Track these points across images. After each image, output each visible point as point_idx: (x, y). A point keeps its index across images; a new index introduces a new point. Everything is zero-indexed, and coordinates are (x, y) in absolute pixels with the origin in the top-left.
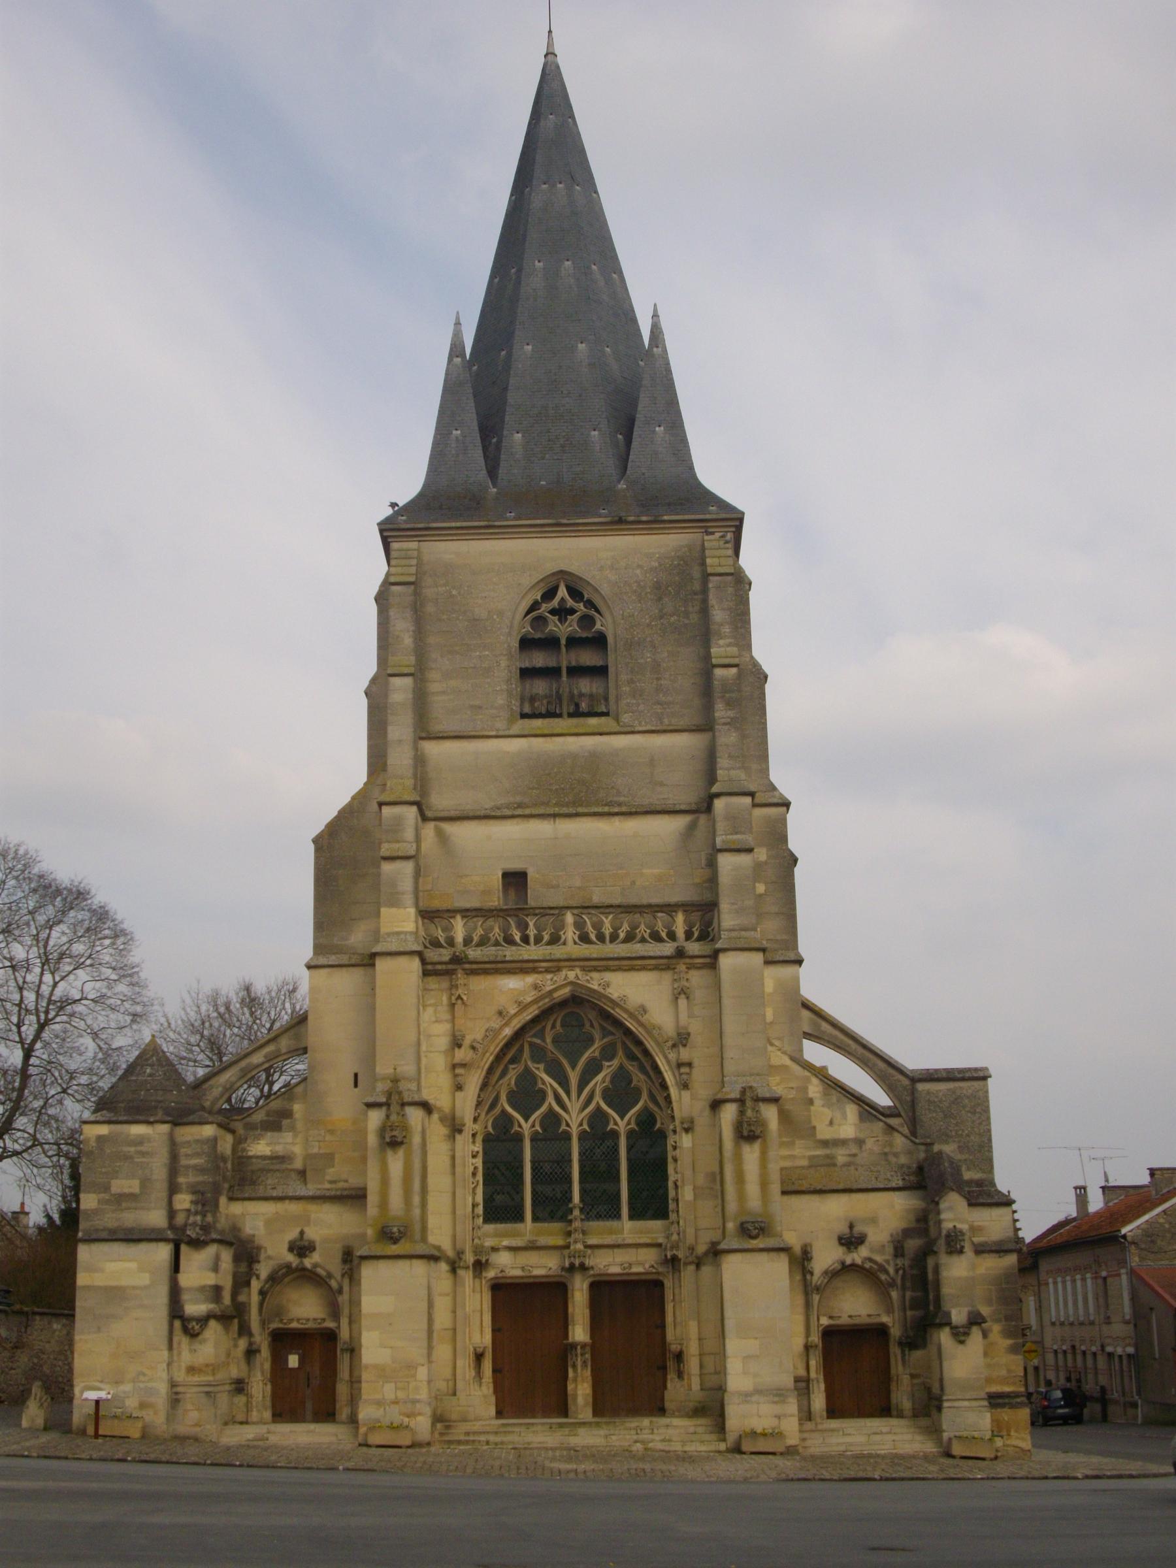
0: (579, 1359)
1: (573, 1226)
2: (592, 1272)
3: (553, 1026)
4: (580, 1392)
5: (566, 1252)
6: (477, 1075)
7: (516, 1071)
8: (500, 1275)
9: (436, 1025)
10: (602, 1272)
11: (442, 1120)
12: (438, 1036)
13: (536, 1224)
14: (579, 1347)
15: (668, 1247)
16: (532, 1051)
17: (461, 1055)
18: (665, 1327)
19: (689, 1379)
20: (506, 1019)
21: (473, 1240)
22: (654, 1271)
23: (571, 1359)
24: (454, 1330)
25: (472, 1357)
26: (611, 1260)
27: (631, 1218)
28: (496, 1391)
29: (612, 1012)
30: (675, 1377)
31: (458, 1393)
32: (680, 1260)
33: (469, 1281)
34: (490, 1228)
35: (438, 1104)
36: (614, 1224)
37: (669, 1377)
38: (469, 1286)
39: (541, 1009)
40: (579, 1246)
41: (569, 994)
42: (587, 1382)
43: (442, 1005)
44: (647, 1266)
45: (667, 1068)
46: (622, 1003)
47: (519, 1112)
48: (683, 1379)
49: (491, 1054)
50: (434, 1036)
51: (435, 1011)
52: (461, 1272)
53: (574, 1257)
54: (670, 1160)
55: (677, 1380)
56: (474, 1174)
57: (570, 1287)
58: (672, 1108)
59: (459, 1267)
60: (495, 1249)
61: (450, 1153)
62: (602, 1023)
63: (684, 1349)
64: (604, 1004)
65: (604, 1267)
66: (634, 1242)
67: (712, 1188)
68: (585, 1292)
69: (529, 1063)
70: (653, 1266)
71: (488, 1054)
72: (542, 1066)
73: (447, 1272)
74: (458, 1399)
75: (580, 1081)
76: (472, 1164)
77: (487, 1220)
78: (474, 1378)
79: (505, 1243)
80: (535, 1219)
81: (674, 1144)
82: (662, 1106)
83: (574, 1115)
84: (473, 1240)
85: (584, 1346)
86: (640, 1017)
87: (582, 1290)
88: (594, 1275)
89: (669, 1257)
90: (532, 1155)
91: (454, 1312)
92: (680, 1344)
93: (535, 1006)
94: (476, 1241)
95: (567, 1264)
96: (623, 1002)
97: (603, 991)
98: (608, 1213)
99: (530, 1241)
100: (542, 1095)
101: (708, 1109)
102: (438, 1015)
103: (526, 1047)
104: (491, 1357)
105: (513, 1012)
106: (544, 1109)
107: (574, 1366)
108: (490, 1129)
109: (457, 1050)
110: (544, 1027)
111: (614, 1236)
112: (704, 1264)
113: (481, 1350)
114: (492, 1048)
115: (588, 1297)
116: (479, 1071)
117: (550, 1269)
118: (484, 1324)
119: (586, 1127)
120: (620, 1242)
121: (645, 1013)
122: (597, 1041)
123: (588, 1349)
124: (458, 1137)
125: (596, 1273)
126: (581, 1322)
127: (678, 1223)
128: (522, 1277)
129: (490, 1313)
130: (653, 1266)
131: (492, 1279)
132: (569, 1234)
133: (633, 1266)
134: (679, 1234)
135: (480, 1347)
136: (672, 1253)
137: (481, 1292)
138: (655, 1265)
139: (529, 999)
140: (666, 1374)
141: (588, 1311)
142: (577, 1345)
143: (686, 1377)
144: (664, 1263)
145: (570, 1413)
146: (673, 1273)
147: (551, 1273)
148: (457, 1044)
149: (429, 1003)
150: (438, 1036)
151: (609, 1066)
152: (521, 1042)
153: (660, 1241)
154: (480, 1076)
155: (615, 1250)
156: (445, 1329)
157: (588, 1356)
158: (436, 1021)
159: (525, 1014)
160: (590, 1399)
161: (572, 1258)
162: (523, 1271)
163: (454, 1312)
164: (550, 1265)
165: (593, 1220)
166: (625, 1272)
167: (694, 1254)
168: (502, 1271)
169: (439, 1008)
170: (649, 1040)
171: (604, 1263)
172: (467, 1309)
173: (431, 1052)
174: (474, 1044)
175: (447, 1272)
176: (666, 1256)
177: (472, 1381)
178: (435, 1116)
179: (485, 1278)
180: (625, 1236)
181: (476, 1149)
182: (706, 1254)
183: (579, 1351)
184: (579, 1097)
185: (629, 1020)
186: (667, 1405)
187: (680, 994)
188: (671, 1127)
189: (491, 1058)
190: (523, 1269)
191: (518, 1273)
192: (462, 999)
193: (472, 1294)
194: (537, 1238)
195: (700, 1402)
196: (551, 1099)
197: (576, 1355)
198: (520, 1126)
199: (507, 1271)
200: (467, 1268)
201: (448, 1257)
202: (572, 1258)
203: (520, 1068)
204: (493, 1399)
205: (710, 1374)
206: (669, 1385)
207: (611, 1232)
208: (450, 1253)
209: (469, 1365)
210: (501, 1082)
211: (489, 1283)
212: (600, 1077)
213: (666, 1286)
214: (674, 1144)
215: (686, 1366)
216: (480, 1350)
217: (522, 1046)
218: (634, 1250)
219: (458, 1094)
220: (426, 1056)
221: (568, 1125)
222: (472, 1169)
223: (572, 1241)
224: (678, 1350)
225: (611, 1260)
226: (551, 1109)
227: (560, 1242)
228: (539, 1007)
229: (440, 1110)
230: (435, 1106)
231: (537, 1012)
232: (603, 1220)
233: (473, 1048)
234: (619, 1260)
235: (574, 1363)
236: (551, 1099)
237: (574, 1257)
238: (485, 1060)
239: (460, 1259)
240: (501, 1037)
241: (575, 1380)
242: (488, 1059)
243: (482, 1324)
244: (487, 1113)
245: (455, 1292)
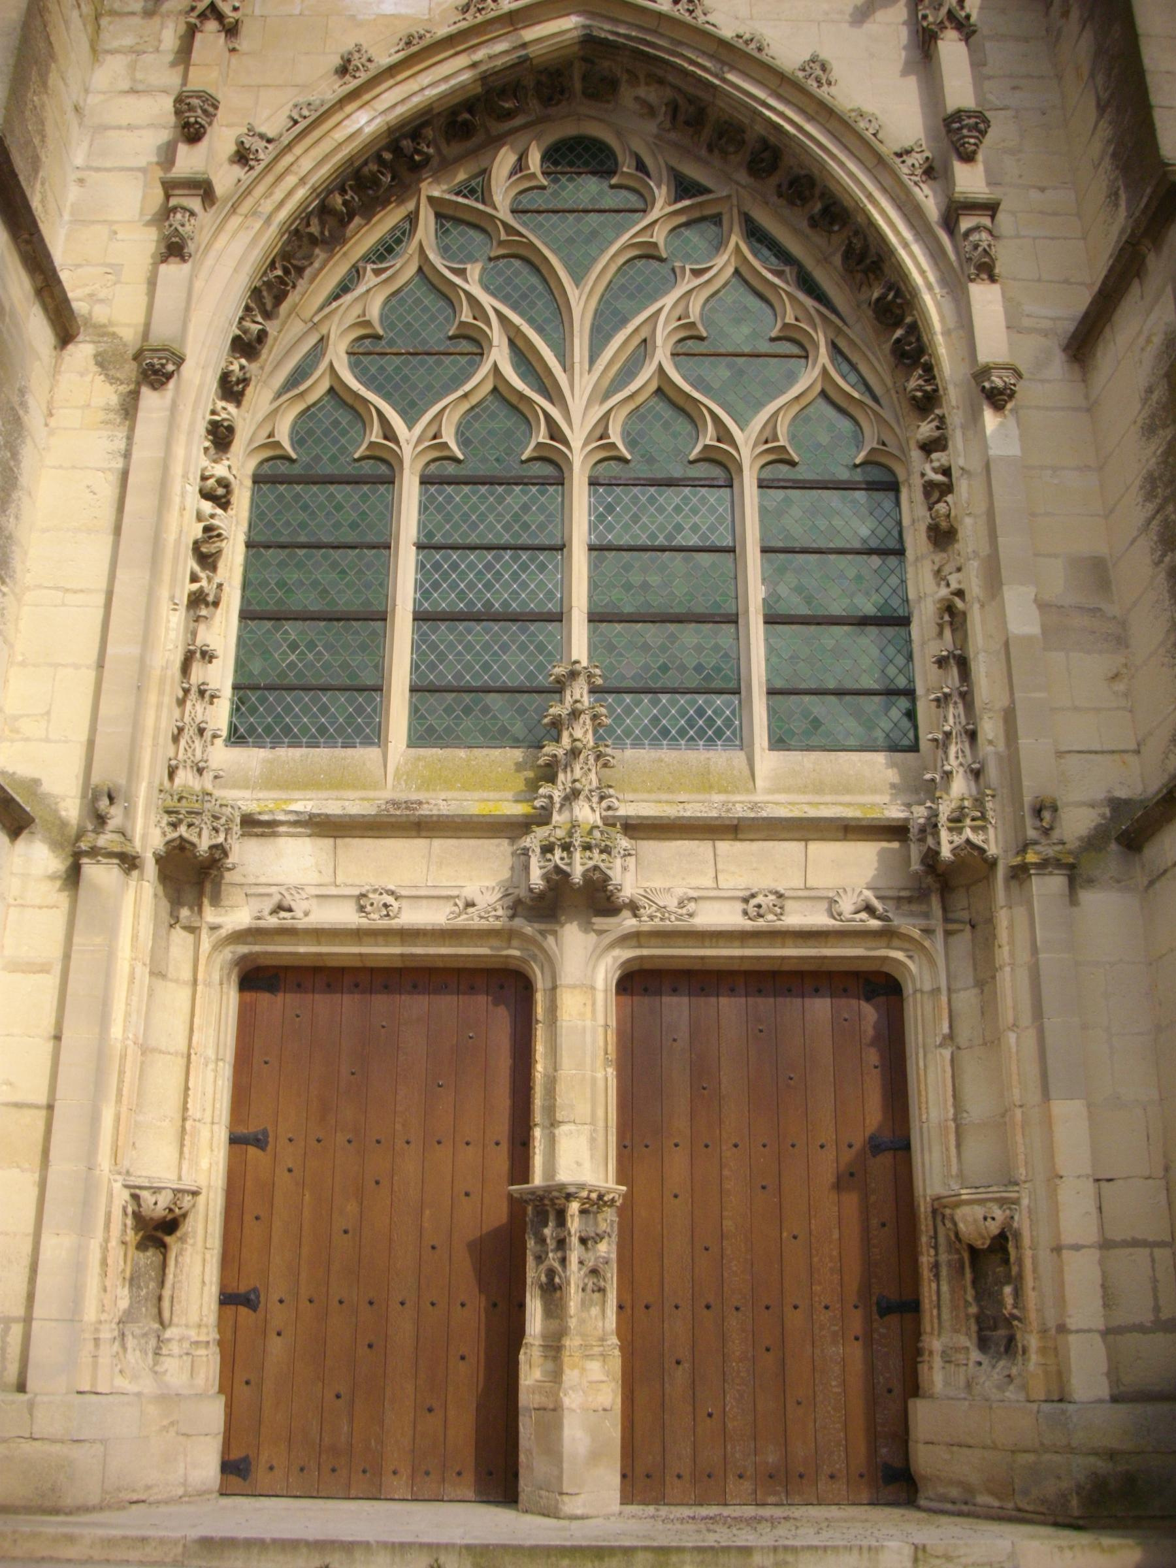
0: (574, 1257)
1: (566, 740)
2: (628, 922)
3: (520, 165)
4: (571, 1400)
5: (534, 840)
6: (245, 238)
7: (384, 276)
8: (272, 921)
9: (132, 100)
10: (671, 923)
11: (102, 362)
12: (130, 127)
13: (422, 752)
14: (574, 1207)
15: (943, 819)
16: (442, 232)
17: (189, 161)
18: (907, 1147)
19: (1054, 1351)
20: (363, 77)
21: (172, 774)
22: (874, 923)
23: (539, 1259)
24: (50, 1107)
25: (121, 1228)
26: (708, 882)
27: (779, 742)
28: (227, 1385)
29: (717, 82)
30: (966, 1341)
31: (30, 1385)
32: (992, 864)
33: (136, 916)
34: (253, 758)
35: (100, 314)
36: (720, 759)
37: (935, 1343)
38: (135, 937)
39: (483, 68)
40: (586, 813)
41: (575, 33)
42: (604, 1356)
43: (157, 50)
44: (847, 906)
45: (908, 235)
46: (751, 49)
47: (387, 397)
48: (1010, 1347)
49: (303, 181)
50: (120, 128)
51: (132, 67)
52: (101, 874)
53: (566, 847)
54: (916, 541)
55: (975, 1355)
56: (207, 559)
57: (541, 983)
58: (929, 369)
59: (94, 852)
60: (252, 825)
61: (119, 464)
62: (674, 163)
63: (1022, 1222)
64: (692, 62)
65: (681, 904)
66: (796, 813)
67: (1095, 611)
68: (600, 996)
69: (433, 256)
70: (869, 909)
71: (291, 180)
72: (474, 271)
73: (52, 878)
74: (31, 1406)
75: (598, 314)
76: (199, 518)
77: (236, 737)
78: (126, 1319)
79: (305, 804)
80: (421, 736)
81: (940, 478)
82: (878, 390)
83: (576, 405)
84: (172, 774)
85: (594, 1204)
86: (812, 85)
87: (593, 988)
88: (635, 938)
89: (946, 852)
90: (422, 525)
91: (58, 1038)
92: (1002, 1202)
93: (462, 61)
94: (184, 777)
95: (536, 877)
96: (753, 46)
97: (687, 18)
98: (691, 723)
99: (395, 804)
100: (475, 343)
101: (1059, 359)
102: (139, 76)
103: (427, 218)
104: (215, 1242)
105: (385, 60)
106: (479, 380)
107: (552, 1289)
108: (283, 435)
109: (182, 149)
110: (485, 172)
111: (718, 798)
112: (1090, 882)
113: (164, 1200)
114: (306, 164)
115: (613, 1023)
116: (258, 225)
117: (470, 904)
118: (194, 1110)
119: (615, 436)
120: (740, 811)
121: (829, 83)
122: (659, 203)
123: (608, 1219)
124: (150, 398)
125: (647, 925)
126: (583, 1109)
127: (972, 736)
128: (358, 934)
129: (226, 1070)
130: (869, 909)
131: (239, 936)
132: (549, 773)
133: (789, 905)
134: (976, 774)
135: (156, 1190)
136: (959, 840)
137: (195, 982)
138: (878, 905)
139: (442, 31)
140: (917, 1334)
141: (611, 1072)
142: (569, 1197)
143: (1033, 1342)
144: (910, 900)
145: (525, 1486)
146: (948, 933)
147: (471, 920)
148: (187, 125)
149: (115, 44)
150: (130, 127)
151: (697, 273)
152: (410, 206)
153: (895, 813)
154: (254, 240)
155: (724, 846)
156: (18, 1105)
157: (606, 1249)
158: (133, 91)
159: (426, 79)
160: (614, 1432)
161: (558, 853)
162: (362, 909)
163: (58, 1038)
164: (470, 890)
165: (638, 743)
166: (761, 923)
167: (1056, 835)
168: (280, 908)
169: (149, 58)
170: (843, 157)
171: (680, 892)
172: (116, 1031)
173: (98, 170)
174: (248, 142)
175: (52, 878)
176: (931, 858)
177: (108, 1333)
178: (82, 351)
179: (214, 928)
180: (758, 797)
181: (220, 470)
182: (1094, 842)
183: (575, 1225)
184: (592, 361)
185: (772, 102)
186: (924, 1459)
187: (942, 27)
188: (926, 430)
189: (301, 193)
190: (361, 902)
191: (345, 916)
192: (220, 16)
193: (142, 972)
194: (421, 796)
195: (1112, 1455)
196: (499, 354)
197: (562, 1244)
198: (389, 434)
199: (299, 907)
200: (129, 862)
201: (64, 824)
202: (558, 853)
203: (405, 268)
204: (214, 1413)
205: (1141, 1329)
206: (936, 1376)
207: (705, 783)
208: (71, 810)
209: (104, 1263)
210: (334, 305)
211: (228, 954)
212: (669, 300)
213: (908, 989)
214: (940, 478)
215: (1031, 1298)
216: (157, 1205)
217: (412, 219)
218: (791, 849)
219: (173, 271)
220: (81, 181)
221: (555, 433)
222: (197, 531)
223: (557, 796)
224: (994, 1228)
225: (708, 882)
226: (500, 392)
227: (520, 809)
228: (474, 65)
229: (102, 332)
230: (87, 321)
231: (465, 76)
232: (674, 744)
233: (242, 157)
234: (737, 880)
235: (551, 1273)
236: (499, 354)
237: (566, 847)
238: (279, 194)
239: (101, 820)
240: (339, 135)
241: (554, 1347)
242: (290, 194)
243: (185, 1109)
244: (279, 395)
245: (67, 957)
